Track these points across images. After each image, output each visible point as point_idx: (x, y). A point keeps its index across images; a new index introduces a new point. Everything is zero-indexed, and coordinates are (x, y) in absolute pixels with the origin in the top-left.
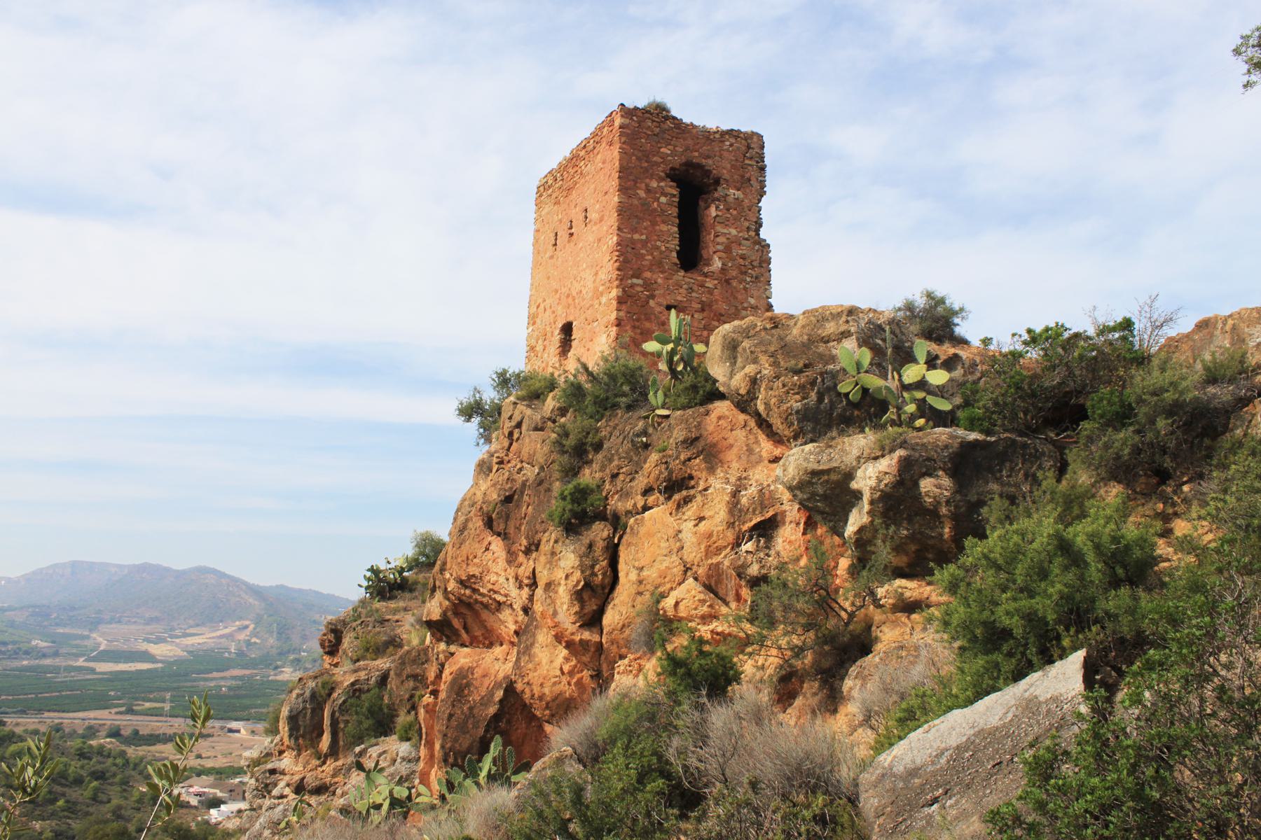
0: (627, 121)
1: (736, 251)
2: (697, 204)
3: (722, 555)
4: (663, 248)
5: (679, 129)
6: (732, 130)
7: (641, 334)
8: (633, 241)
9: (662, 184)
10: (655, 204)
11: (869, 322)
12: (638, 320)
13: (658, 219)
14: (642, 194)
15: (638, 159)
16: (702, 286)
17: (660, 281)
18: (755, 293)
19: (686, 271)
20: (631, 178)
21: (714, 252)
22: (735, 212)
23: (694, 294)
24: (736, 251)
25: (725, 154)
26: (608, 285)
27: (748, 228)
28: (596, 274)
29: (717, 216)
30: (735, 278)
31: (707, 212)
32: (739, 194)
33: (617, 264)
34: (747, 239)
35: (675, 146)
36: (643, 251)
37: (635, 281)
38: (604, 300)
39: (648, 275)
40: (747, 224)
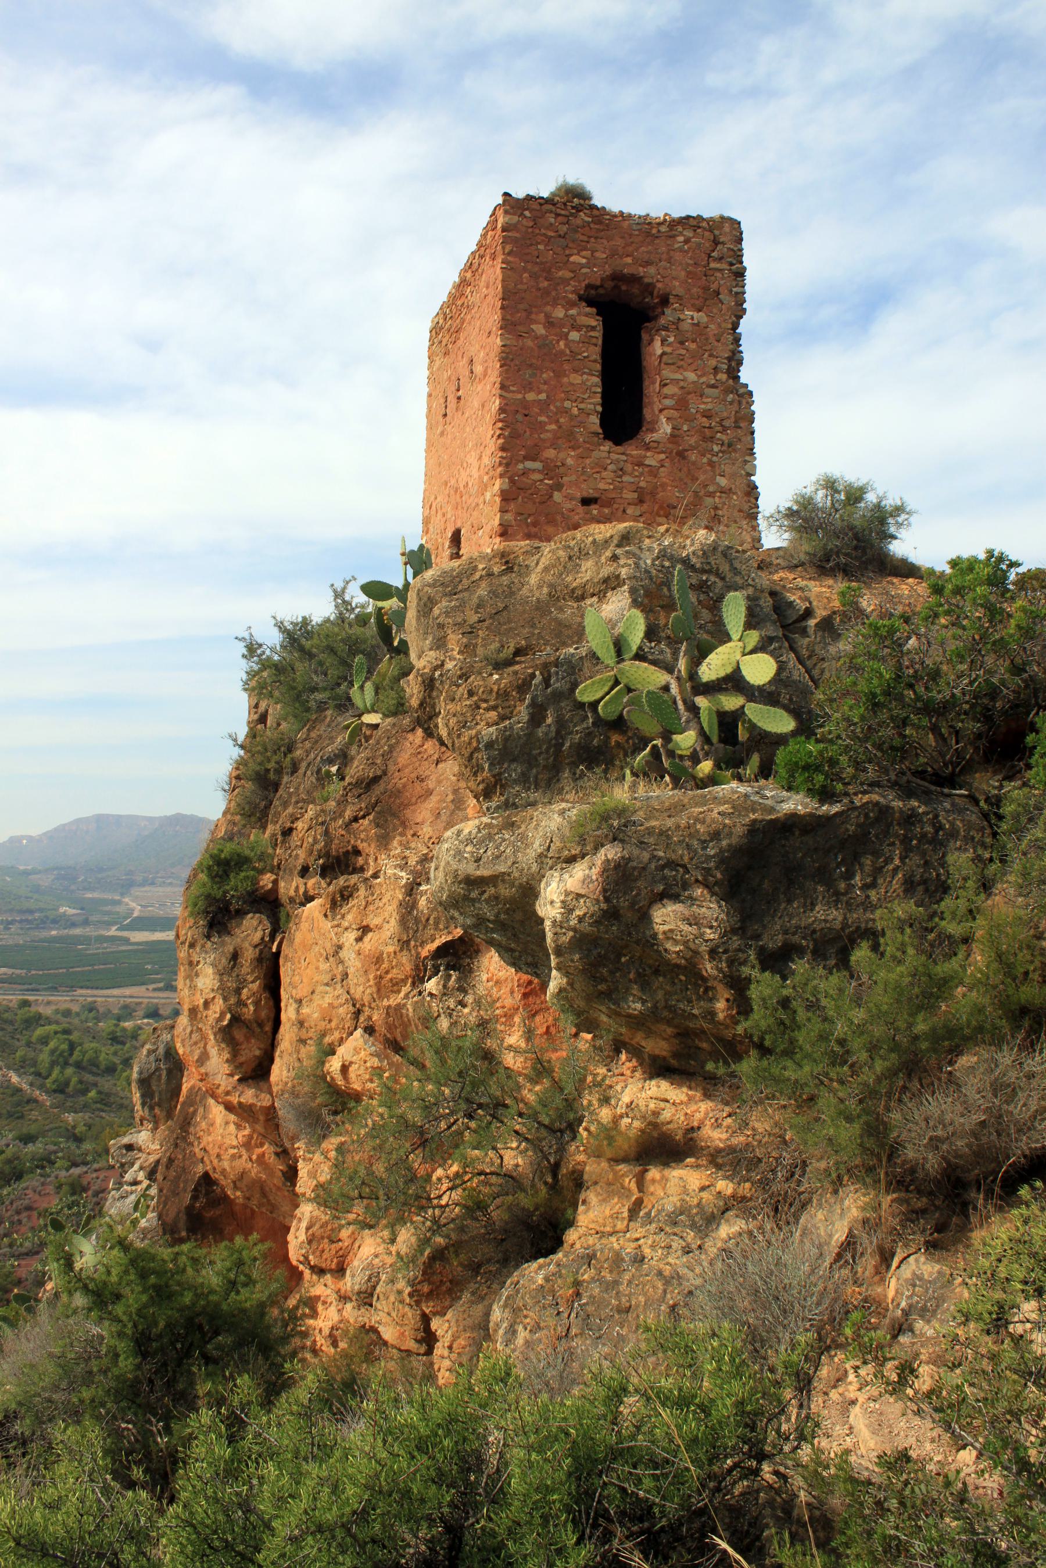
0: (515, 219)
1: (696, 405)
2: (639, 338)
3: (402, 995)
4: (575, 411)
5: (600, 222)
6: (688, 217)
8: (525, 404)
9: (571, 312)
10: (562, 343)
11: (663, 554)
12: (535, 524)
13: (566, 366)
14: (540, 329)
15: (534, 276)
16: (640, 464)
17: (570, 461)
18: (728, 469)
19: (618, 442)
20: (521, 306)
21: (661, 411)
22: (693, 346)
23: (625, 479)
24: (696, 405)
25: (678, 256)
26: (491, 473)
27: (716, 370)
28: (480, 458)
29: (664, 354)
31: (650, 349)
32: (700, 317)
33: (501, 441)
34: (713, 386)
35: (593, 252)
36: (543, 419)
37: (529, 464)
38: (488, 495)
39: (551, 453)
40: (713, 362)
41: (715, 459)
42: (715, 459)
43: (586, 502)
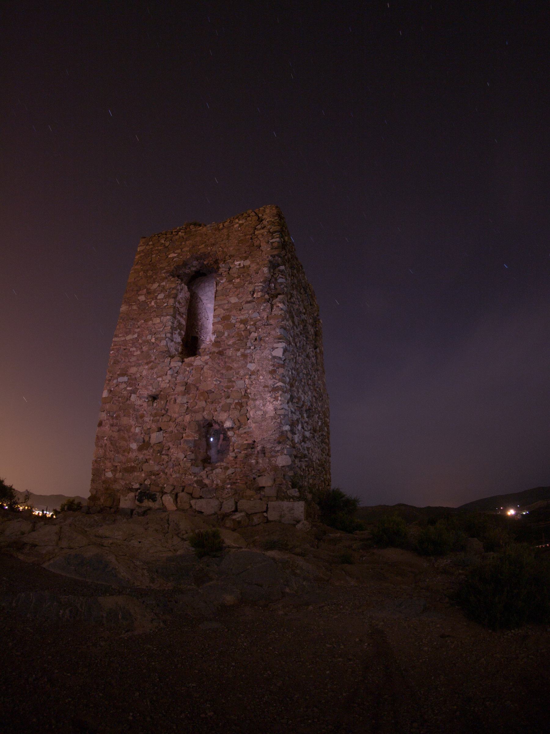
0: (144, 247)
4: (153, 340)
7: (119, 431)
9: (164, 283)
32: (247, 263)
35: (181, 249)
37: (121, 379)
39: (133, 370)
43: (154, 398)
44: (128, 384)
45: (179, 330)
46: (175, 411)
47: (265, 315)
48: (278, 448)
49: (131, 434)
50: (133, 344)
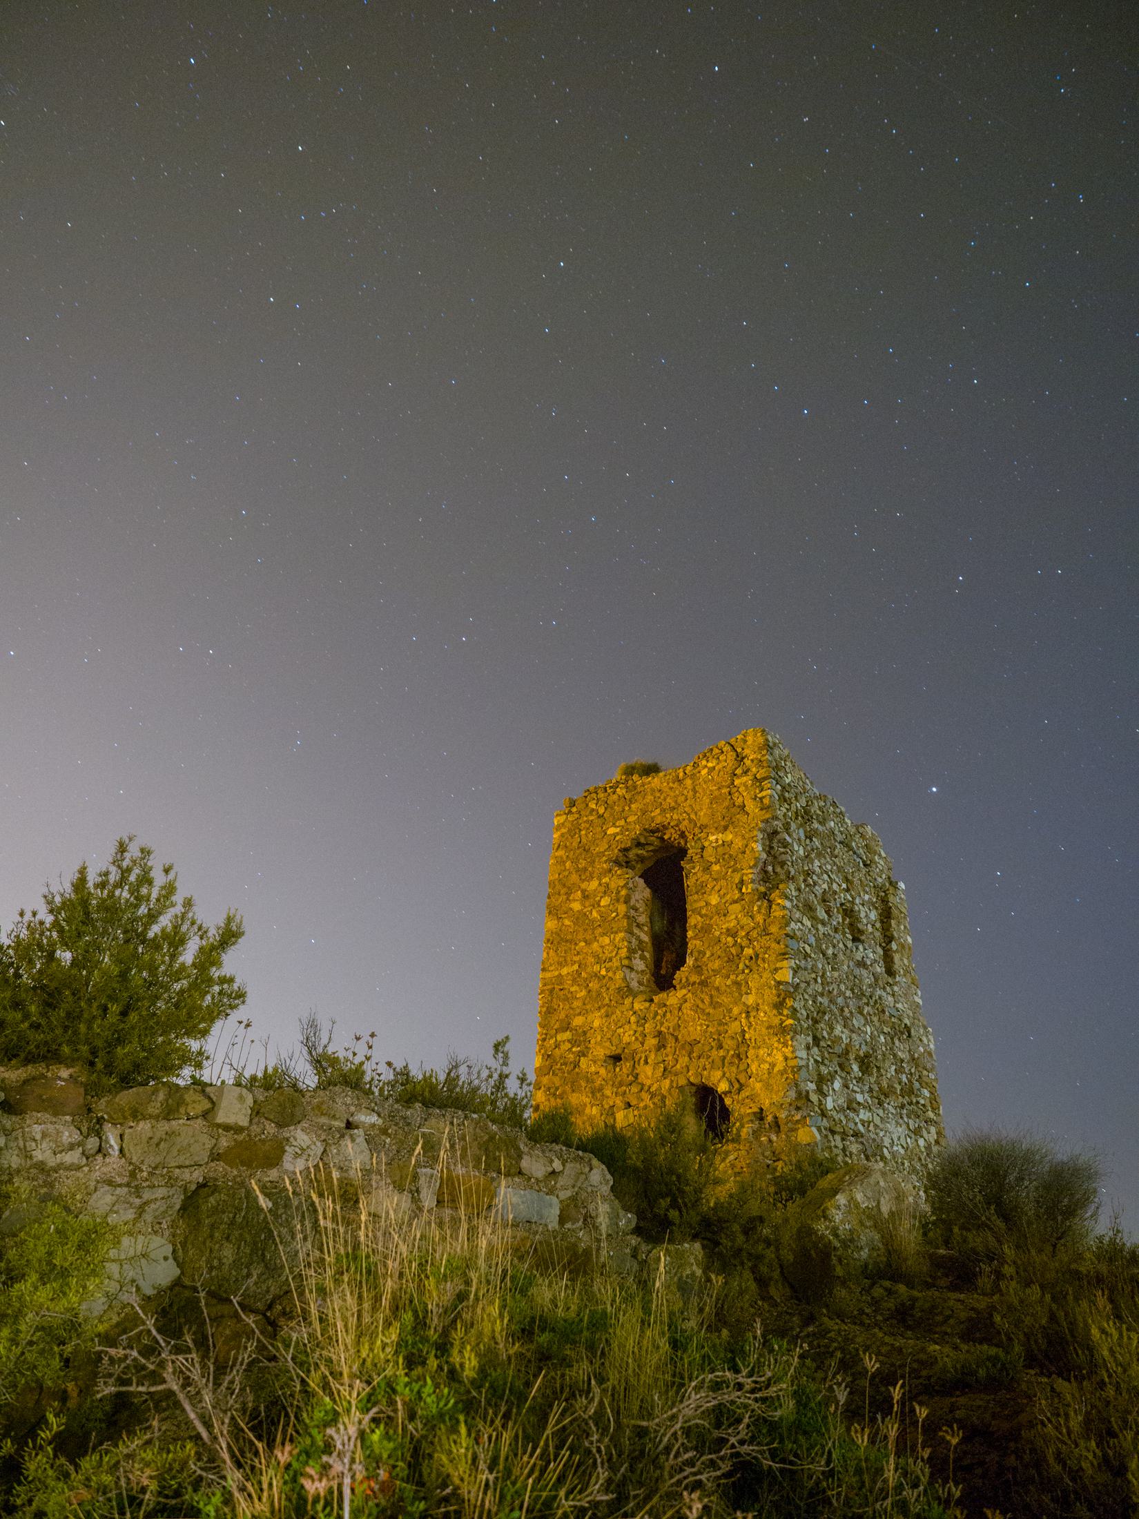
4: (603, 972)
10: (595, 914)
14: (576, 906)
17: (596, 1024)
30: (716, 972)
32: (729, 837)
39: (578, 1021)
41: (741, 977)
42: (741, 977)
43: (616, 1059)
44: (573, 1042)
45: (640, 952)
46: (647, 1073)
47: (760, 918)
48: (797, 1117)
49: (585, 1118)
50: (574, 980)
